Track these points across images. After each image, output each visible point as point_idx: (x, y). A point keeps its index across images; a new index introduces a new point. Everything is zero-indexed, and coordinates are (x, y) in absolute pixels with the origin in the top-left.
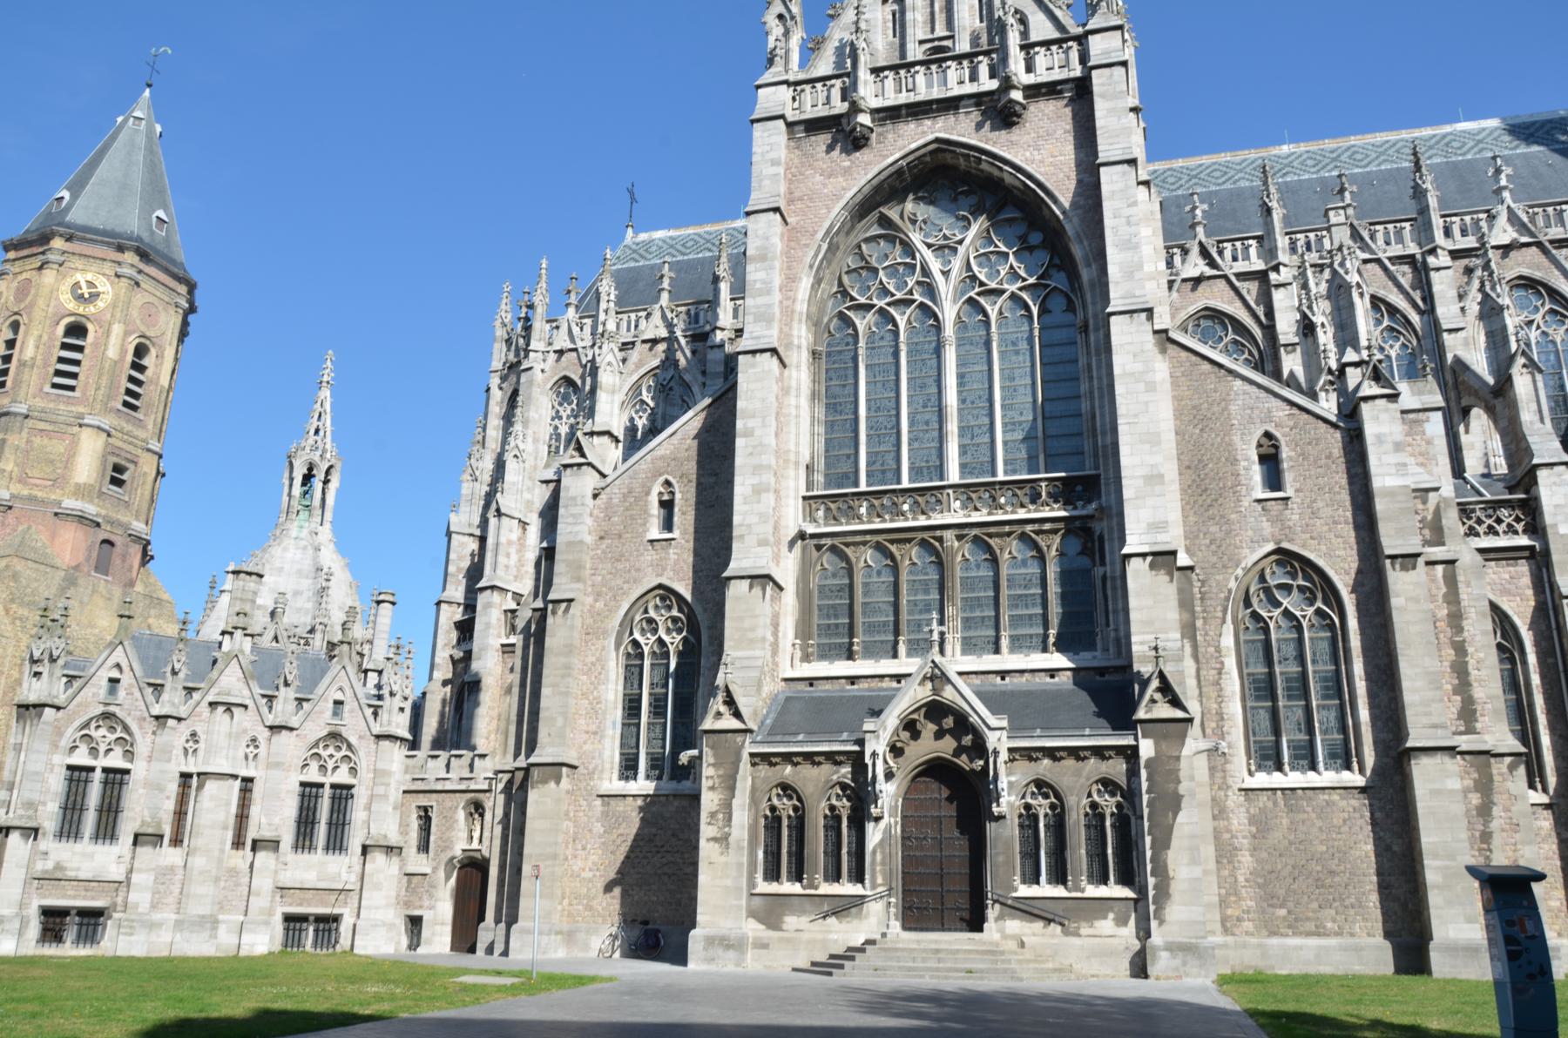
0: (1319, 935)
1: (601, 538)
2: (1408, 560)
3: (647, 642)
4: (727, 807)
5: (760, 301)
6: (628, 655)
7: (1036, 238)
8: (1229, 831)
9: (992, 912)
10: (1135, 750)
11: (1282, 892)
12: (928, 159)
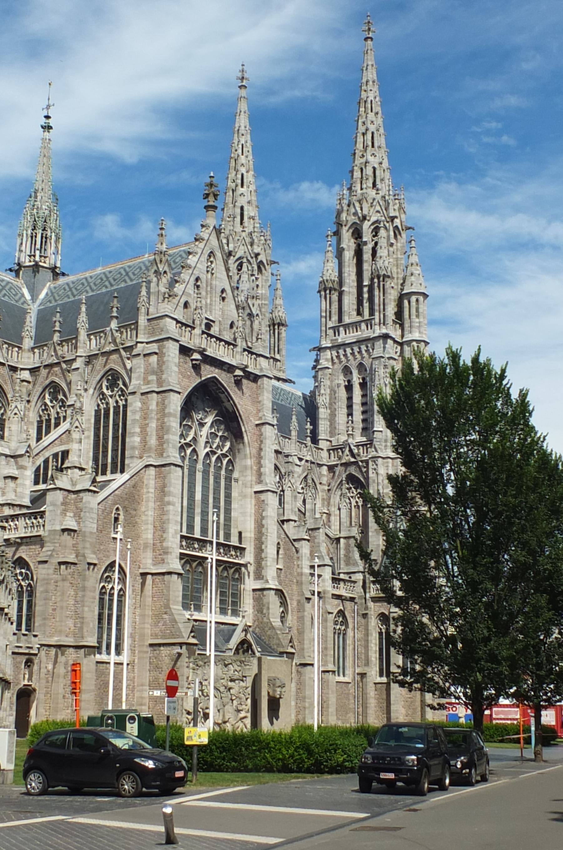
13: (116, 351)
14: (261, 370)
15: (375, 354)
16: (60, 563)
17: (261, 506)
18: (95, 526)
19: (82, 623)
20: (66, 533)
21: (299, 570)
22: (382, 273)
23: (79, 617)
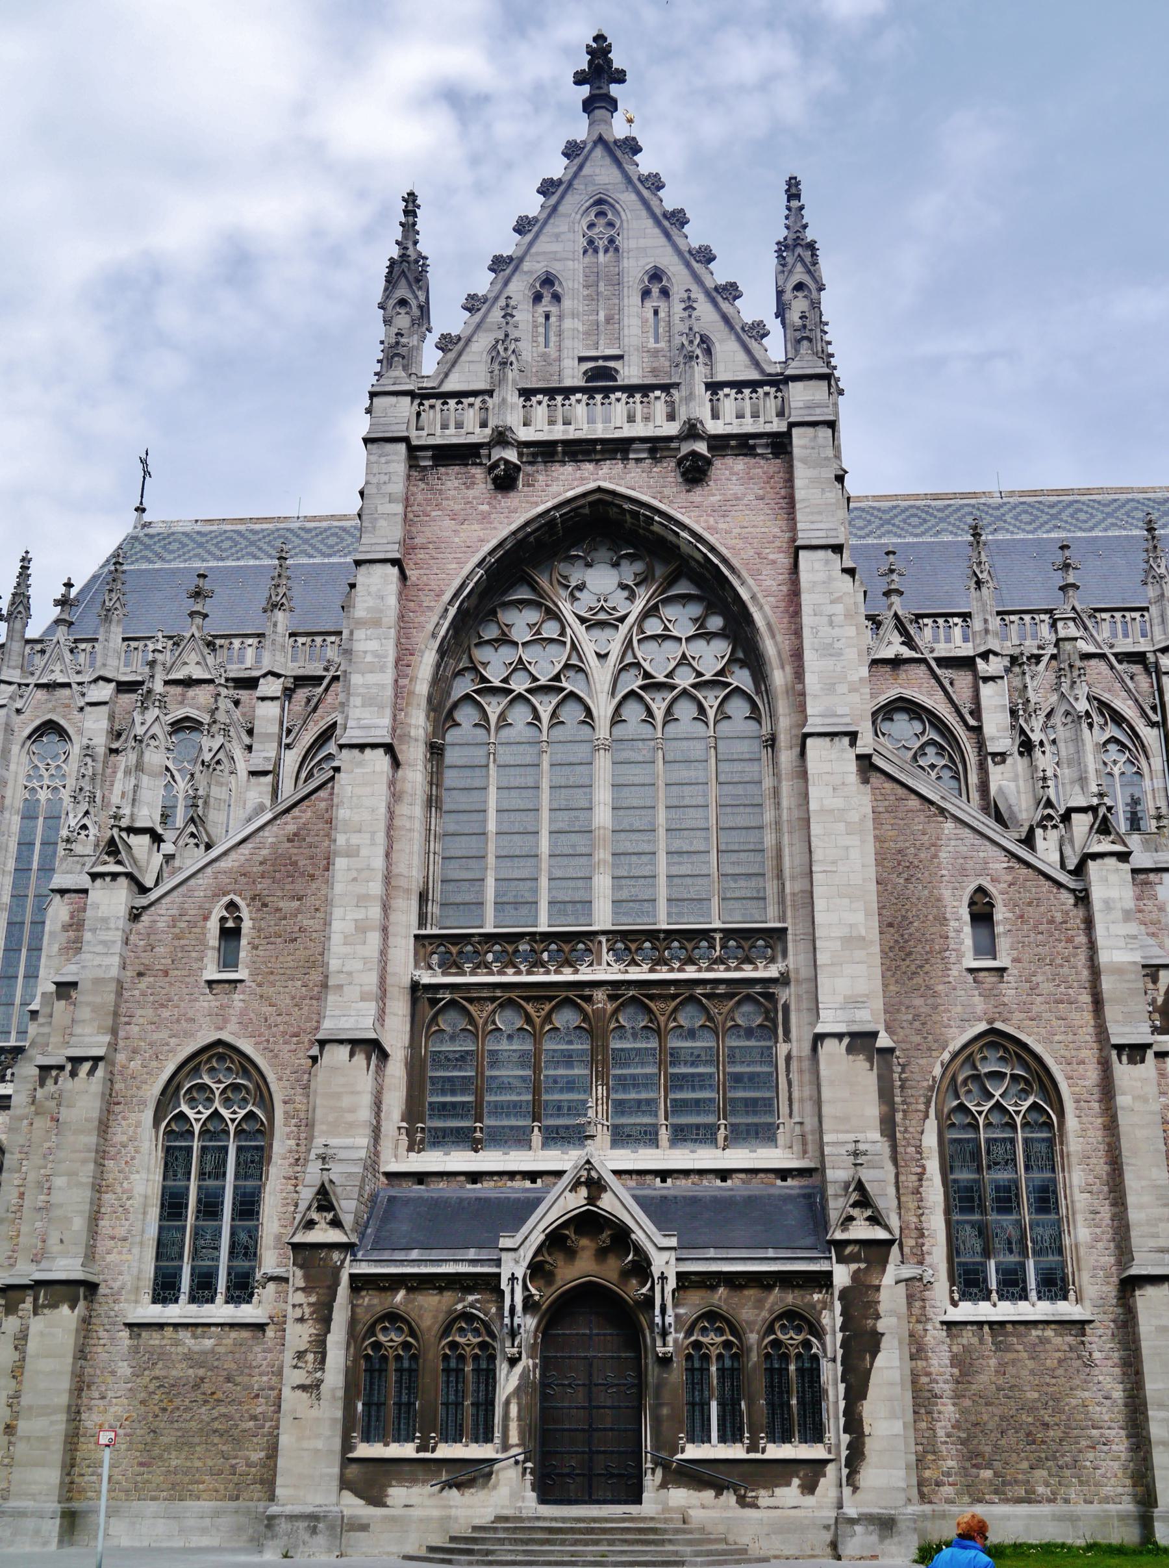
0: (1029, 1501)
1: (140, 974)
2: (1136, 1052)
3: (197, 1116)
4: (320, 1345)
5: (371, 678)
6: (169, 1133)
7: (715, 623)
8: (928, 1374)
9: (651, 1481)
10: (829, 1274)
11: (988, 1449)
12: (586, 511)
18: (116, 960)
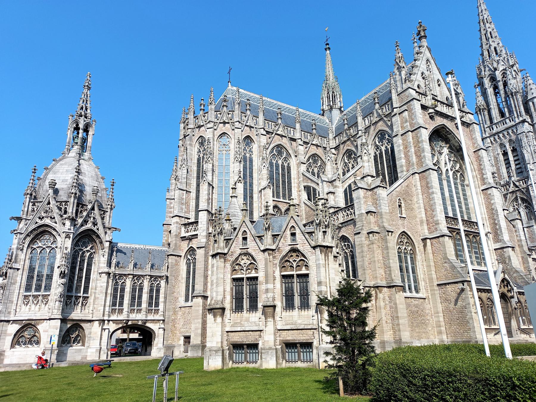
13: (381, 119)
14: (471, 120)
15: (519, 132)
16: (368, 233)
17: (488, 199)
18: (388, 208)
19: (390, 271)
20: (369, 214)
21: (518, 238)
22: (514, 91)
23: (388, 268)
